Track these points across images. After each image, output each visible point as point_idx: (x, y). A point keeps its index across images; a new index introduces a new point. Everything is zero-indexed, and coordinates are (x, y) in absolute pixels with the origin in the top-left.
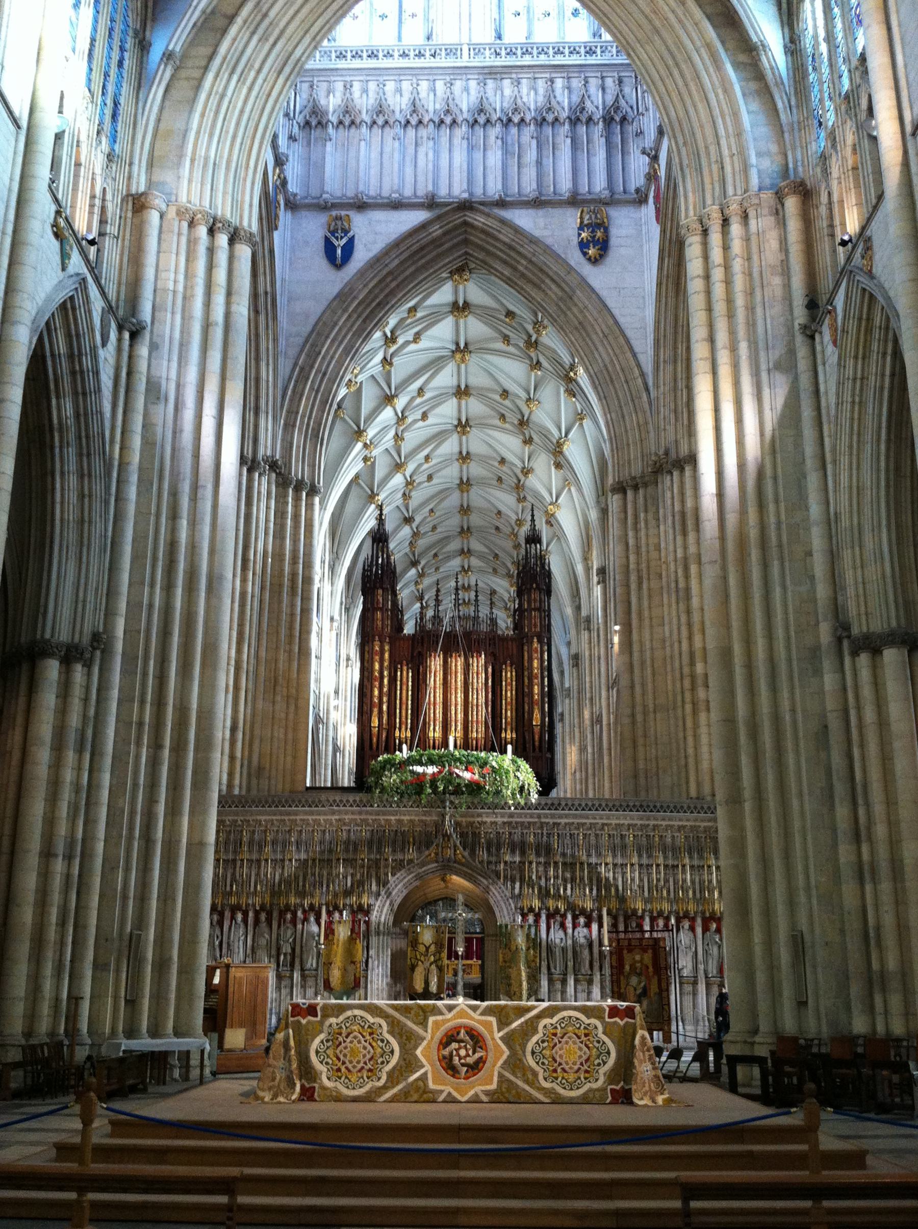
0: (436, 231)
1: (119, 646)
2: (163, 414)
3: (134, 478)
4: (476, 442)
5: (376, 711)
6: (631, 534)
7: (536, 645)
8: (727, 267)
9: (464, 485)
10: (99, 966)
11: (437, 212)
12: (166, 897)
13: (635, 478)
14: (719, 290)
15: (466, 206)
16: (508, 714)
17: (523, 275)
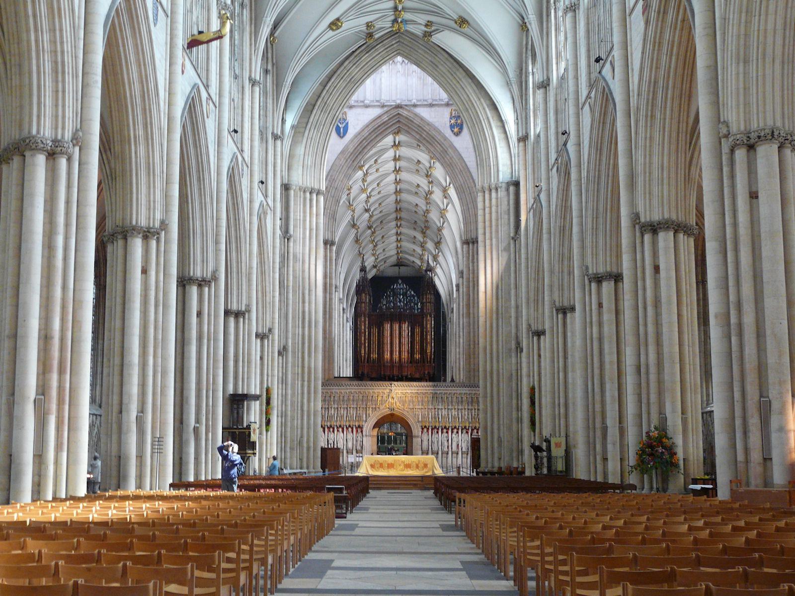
0: (385, 118)
1: (290, 349)
2: (299, 265)
3: (291, 291)
4: (404, 176)
5: (363, 347)
6: (471, 265)
7: (429, 318)
8: (490, 207)
9: (397, 192)
10: (292, 449)
11: (386, 109)
12: (308, 428)
13: (472, 239)
14: (487, 216)
15: (399, 106)
16: (417, 347)
17: (425, 139)
